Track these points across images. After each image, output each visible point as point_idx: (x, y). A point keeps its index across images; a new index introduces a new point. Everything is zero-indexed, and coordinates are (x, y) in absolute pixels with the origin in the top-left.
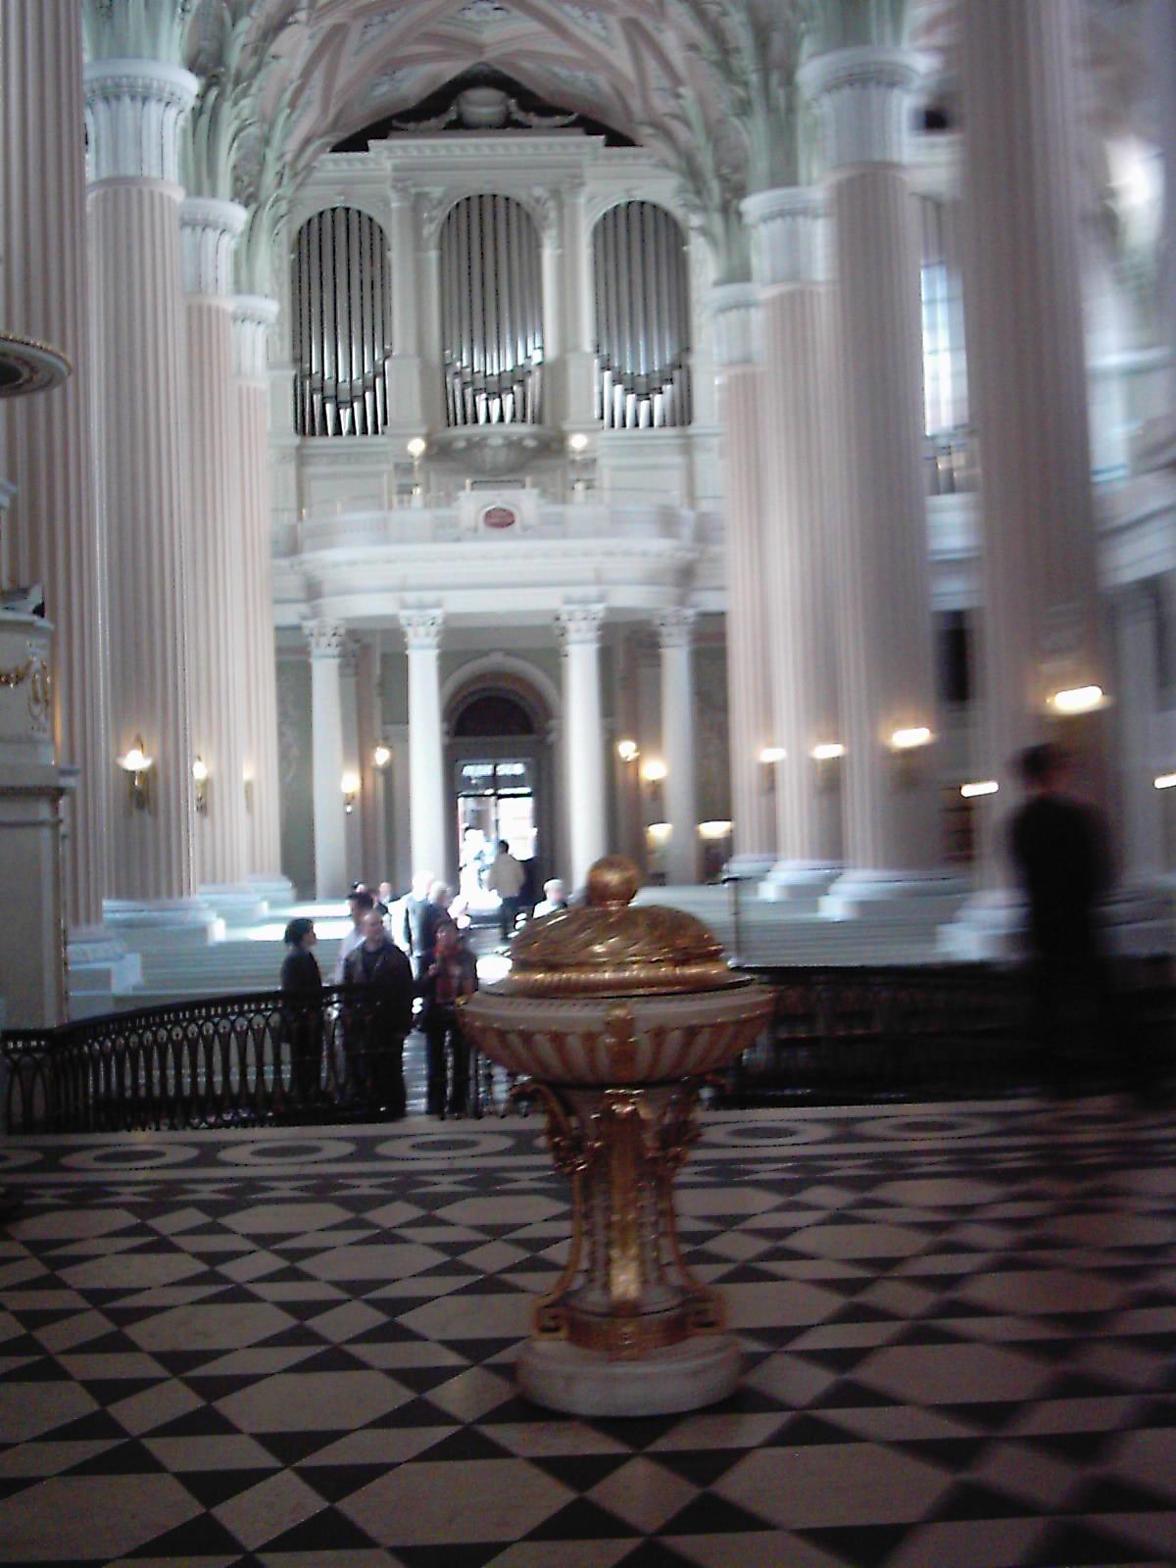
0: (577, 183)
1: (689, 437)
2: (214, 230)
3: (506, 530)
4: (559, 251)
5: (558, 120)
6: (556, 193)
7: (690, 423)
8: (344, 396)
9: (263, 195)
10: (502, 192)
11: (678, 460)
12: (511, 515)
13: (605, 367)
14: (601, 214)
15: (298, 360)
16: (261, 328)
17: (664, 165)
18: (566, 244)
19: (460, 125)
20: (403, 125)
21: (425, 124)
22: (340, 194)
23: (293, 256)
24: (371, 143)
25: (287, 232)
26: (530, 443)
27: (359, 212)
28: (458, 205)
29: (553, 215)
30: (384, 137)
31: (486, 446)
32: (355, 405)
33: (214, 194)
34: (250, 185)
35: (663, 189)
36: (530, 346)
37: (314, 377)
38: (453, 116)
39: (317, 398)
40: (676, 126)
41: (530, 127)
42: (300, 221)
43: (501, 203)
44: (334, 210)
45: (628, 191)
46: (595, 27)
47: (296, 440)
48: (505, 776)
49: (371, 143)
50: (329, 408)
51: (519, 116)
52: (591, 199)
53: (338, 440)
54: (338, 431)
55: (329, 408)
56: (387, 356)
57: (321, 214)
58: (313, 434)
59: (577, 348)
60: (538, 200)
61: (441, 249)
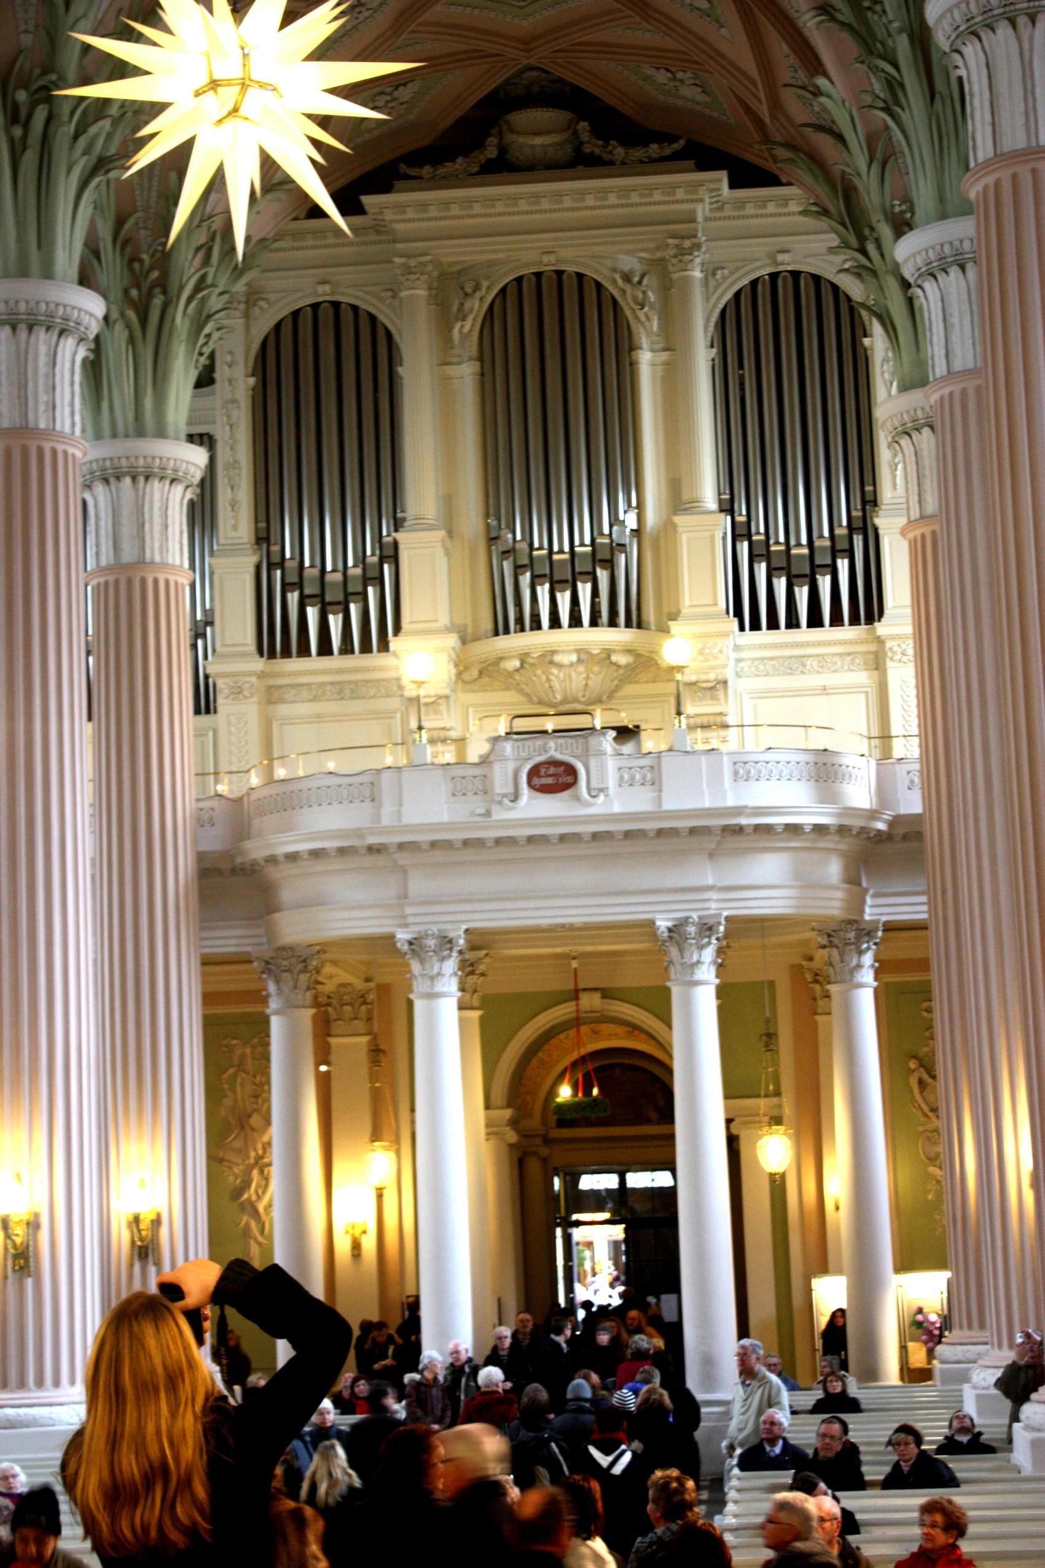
1: (880, 641)
2: (48, 328)
3: (565, 794)
5: (654, 149)
10: (571, 268)
11: (863, 677)
12: (571, 771)
13: (741, 532)
14: (729, 295)
16: (178, 489)
17: (825, 212)
19: (504, 167)
20: (412, 172)
21: (448, 168)
22: (324, 282)
23: (252, 381)
24: (367, 200)
25: (236, 347)
26: (622, 659)
27: (355, 309)
28: (503, 290)
30: (387, 189)
31: (551, 662)
32: (353, 607)
33: (48, 273)
34: (152, 268)
35: (817, 251)
36: (622, 506)
37: (288, 564)
38: (491, 152)
39: (293, 598)
40: (824, 144)
41: (611, 163)
42: (263, 325)
44: (315, 307)
45: (772, 256)
47: (259, 664)
48: (592, 1191)
49: (367, 200)
50: (312, 613)
51: (593, 146)
52: (710, 272)
53: (325, 662)
54: (325, 649)
55: (312, 613)
56: (398, 524)
57: (296, 314)
58: (286, 653)
60: (627, 278)
61: (481, 359)
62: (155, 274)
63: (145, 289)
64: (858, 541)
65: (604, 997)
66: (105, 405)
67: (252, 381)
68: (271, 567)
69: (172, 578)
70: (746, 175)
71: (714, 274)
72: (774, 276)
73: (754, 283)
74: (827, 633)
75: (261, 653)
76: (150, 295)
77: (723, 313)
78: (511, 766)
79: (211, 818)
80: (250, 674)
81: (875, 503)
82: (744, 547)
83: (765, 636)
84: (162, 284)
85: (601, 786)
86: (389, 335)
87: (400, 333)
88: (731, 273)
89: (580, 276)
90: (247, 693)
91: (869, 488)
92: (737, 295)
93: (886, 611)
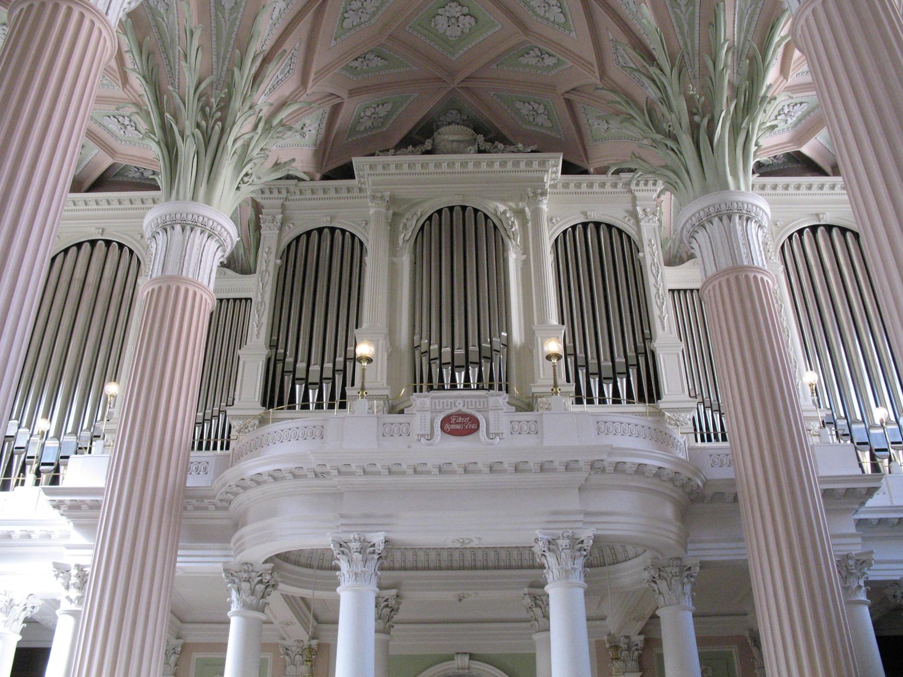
0: (539, 192)
1: (660, 414)
4: (524, 257)
6: (520, 213)
7: (659, 398)
8: (314, 377)
9: (229, 122)
10: (471, 203)
12: (476, 421)
15: (273, 345)
16: (212, 245)
18: (531, 252)
27: (343, 231)
28: (430, 218)
29: (516, 226)
39: (288, 379)
42: (290, 235)
43: (469, 214)
44: (320, 230)
46: (555, 13)
47: (261, 410)
57: (309, 233)
59: (543, 318)
60: (504, 212)
62: (219, 114)
63: (211, 123)
64: (642, 360)
65: (470, 659)
66: (174, 192)
67: (279, 261)
68: (275, 360)
69: (199, 292)
70: (568, 168)
71: (551, 220)
72: (585, 225)
73: (574, 227)
74: (624, 407)
75: (264, 404)
76: (213, 128)
77: (556, 240)
78: (428, 415)
79: (205, 469)
80: (254, 417)
81: (651, 339)
82: (570, 360)
83: (585, 407)
84: (223, 119)
85: (497, 432)
86: (361, 243)
87: (367, 240)
88: (561, 220)
89: (476, 211)
90: (250, 429)
91: (647, 331)
92: (564, 232)
93: (665, 398)
